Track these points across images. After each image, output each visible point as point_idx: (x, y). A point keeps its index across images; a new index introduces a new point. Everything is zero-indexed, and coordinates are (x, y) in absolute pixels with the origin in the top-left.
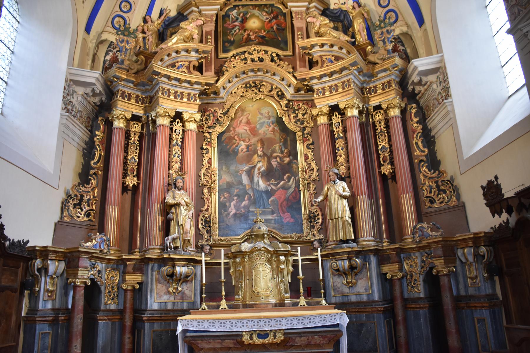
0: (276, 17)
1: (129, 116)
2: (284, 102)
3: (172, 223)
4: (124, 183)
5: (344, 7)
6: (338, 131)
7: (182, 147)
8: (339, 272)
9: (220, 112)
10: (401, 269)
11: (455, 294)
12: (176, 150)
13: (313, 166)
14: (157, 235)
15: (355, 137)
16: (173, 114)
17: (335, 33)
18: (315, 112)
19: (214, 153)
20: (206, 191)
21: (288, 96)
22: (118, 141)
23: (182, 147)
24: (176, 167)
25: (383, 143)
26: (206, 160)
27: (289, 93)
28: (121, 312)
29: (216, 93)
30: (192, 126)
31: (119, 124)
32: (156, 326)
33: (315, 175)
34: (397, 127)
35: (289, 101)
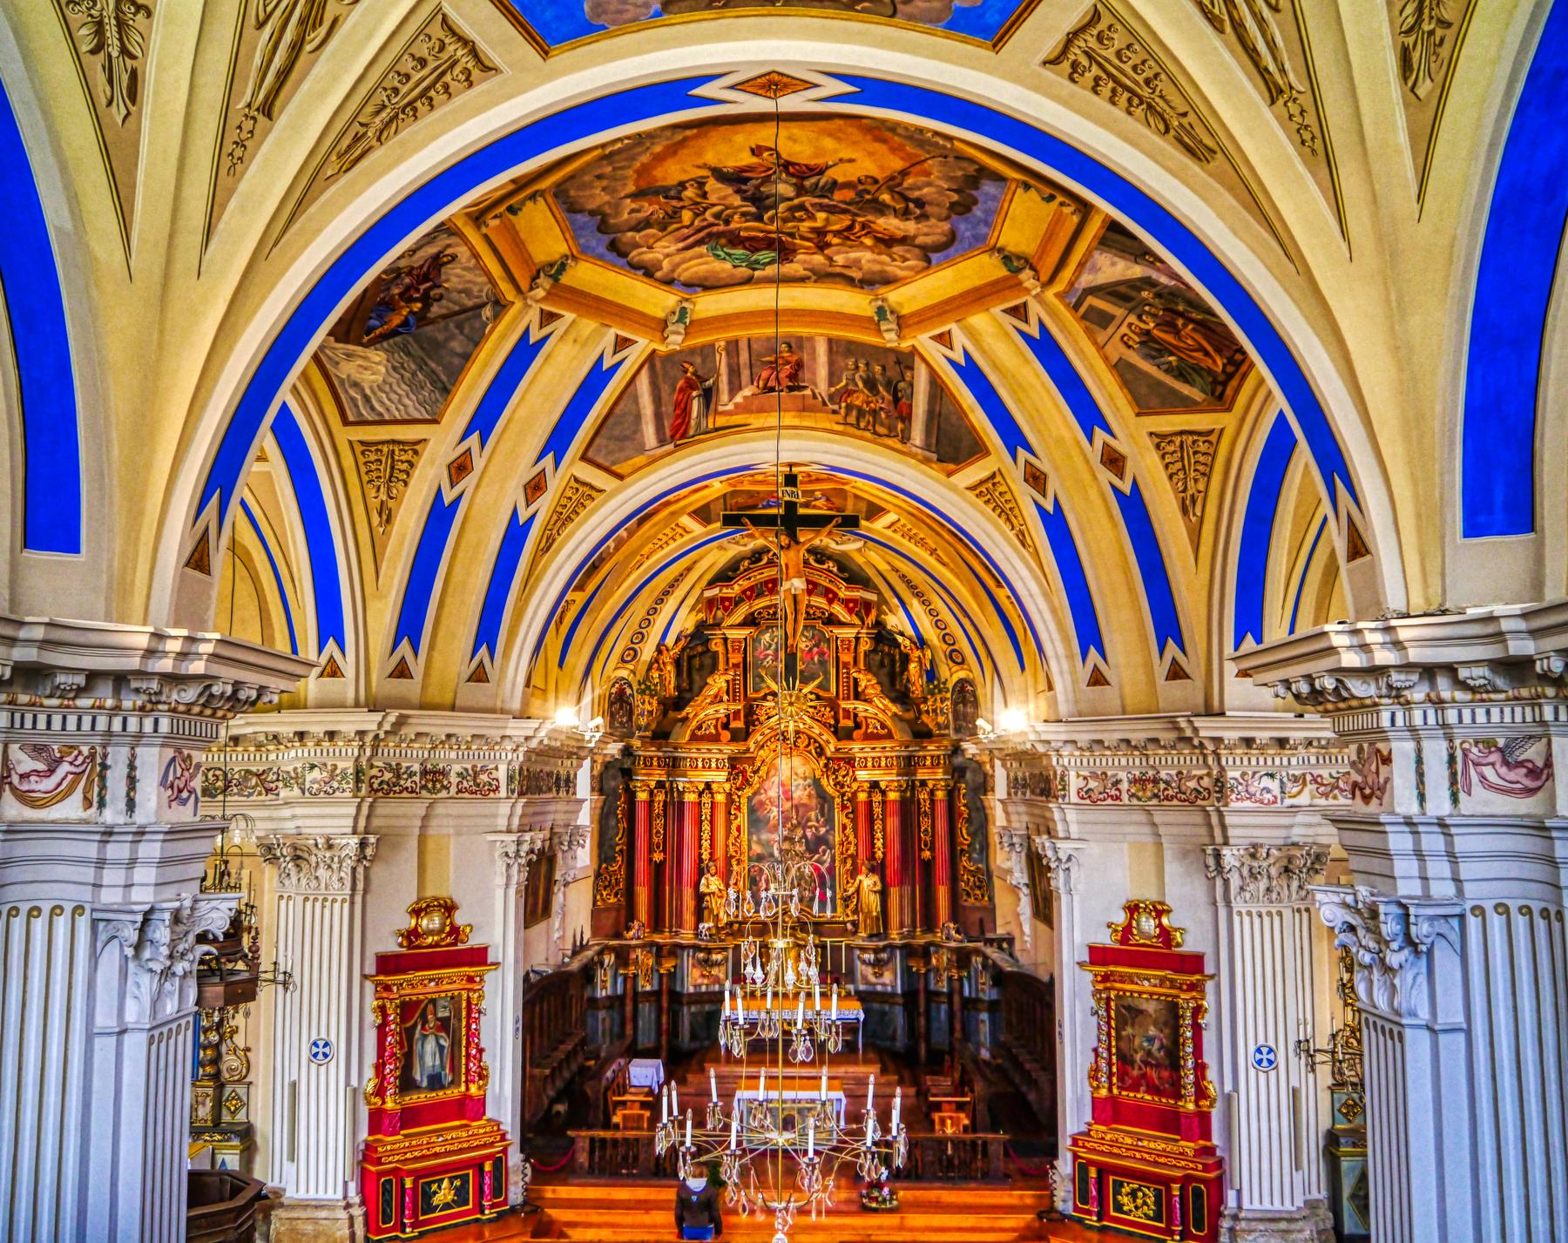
0: (817, 645)
1: (653, 784)
2: (823, 761)
3: (706, 913)
4: (650, 860)
5: (900, 639)
6: (877, 810)
7: (712, 822)
8: (868, 963)
9: (749, 770)
10: (928, 962)
11: (966, 993)
12: (706, 826)
13: (851, 838)
14: (689, 917)
15: (893, 823)
16: (701, 787)
17: (882, 702)
18: (855, 786)
19: (742, 819)
20: (734, 862)
21: (829, 754)
22: (641, 814)
23: (712, 822)
24: (706, 844)
25: (925, 824)
26: (734, 827)
27: (830, 750)
28: (656, 994)
29: (748, 750)
30: (720, 798)
31: (642, 796)
32: (693, 1009)
33: (852, 848)
34: (941, 810)
35: (828, 759)
